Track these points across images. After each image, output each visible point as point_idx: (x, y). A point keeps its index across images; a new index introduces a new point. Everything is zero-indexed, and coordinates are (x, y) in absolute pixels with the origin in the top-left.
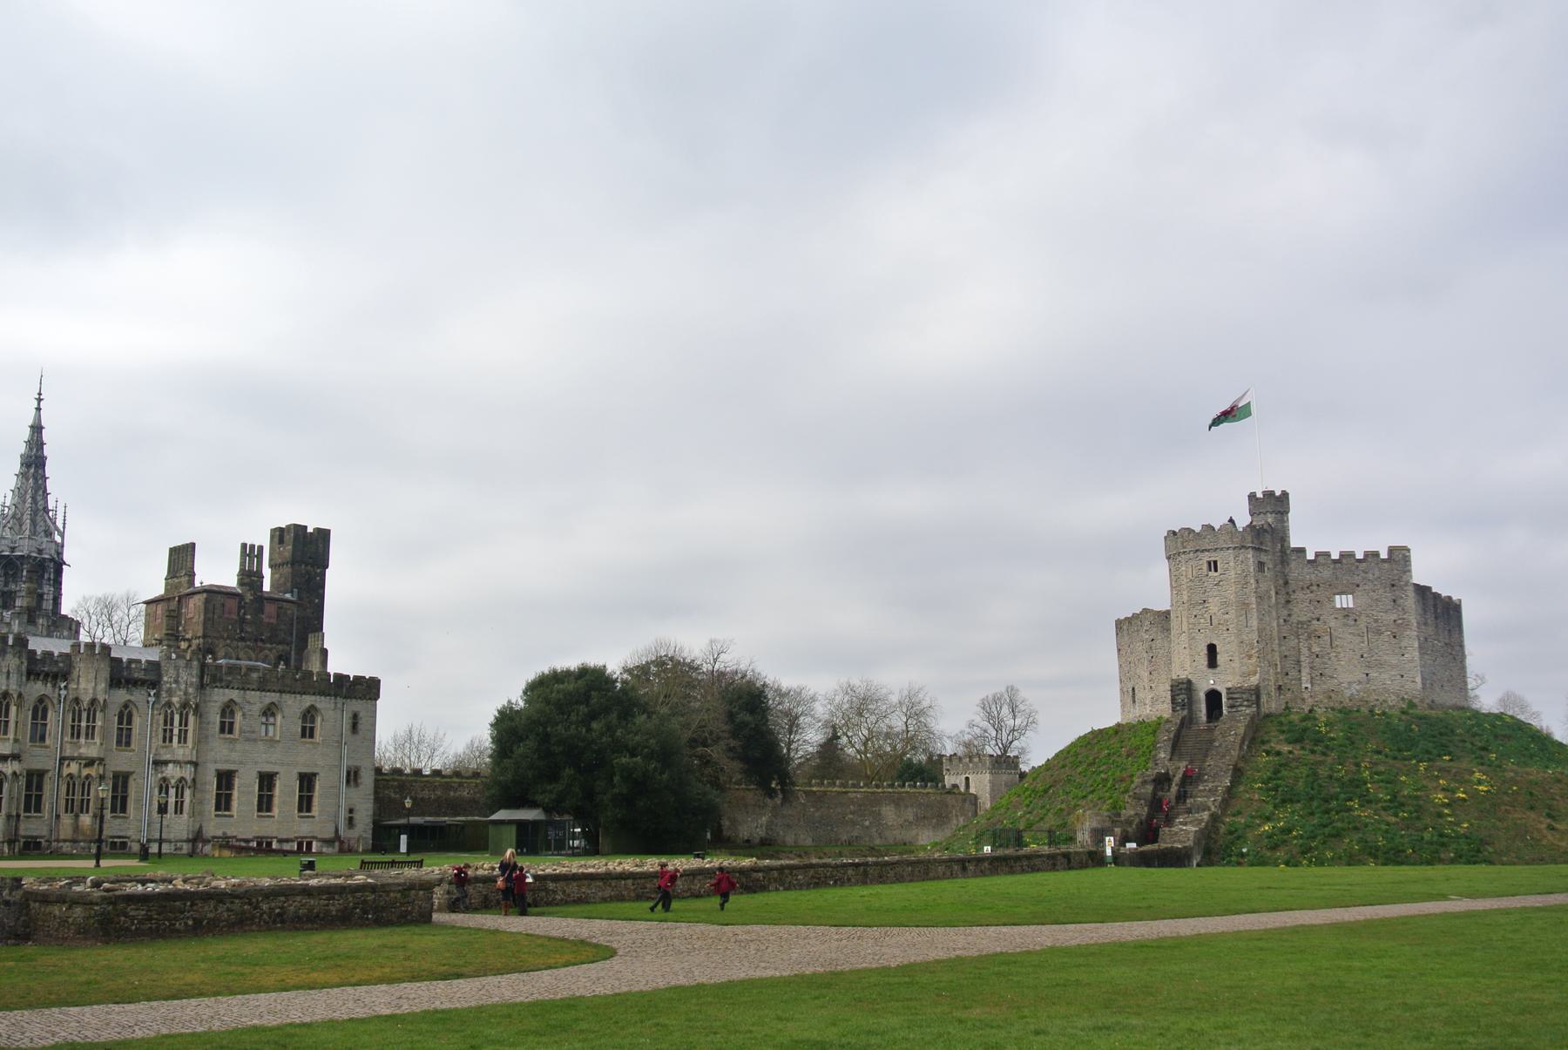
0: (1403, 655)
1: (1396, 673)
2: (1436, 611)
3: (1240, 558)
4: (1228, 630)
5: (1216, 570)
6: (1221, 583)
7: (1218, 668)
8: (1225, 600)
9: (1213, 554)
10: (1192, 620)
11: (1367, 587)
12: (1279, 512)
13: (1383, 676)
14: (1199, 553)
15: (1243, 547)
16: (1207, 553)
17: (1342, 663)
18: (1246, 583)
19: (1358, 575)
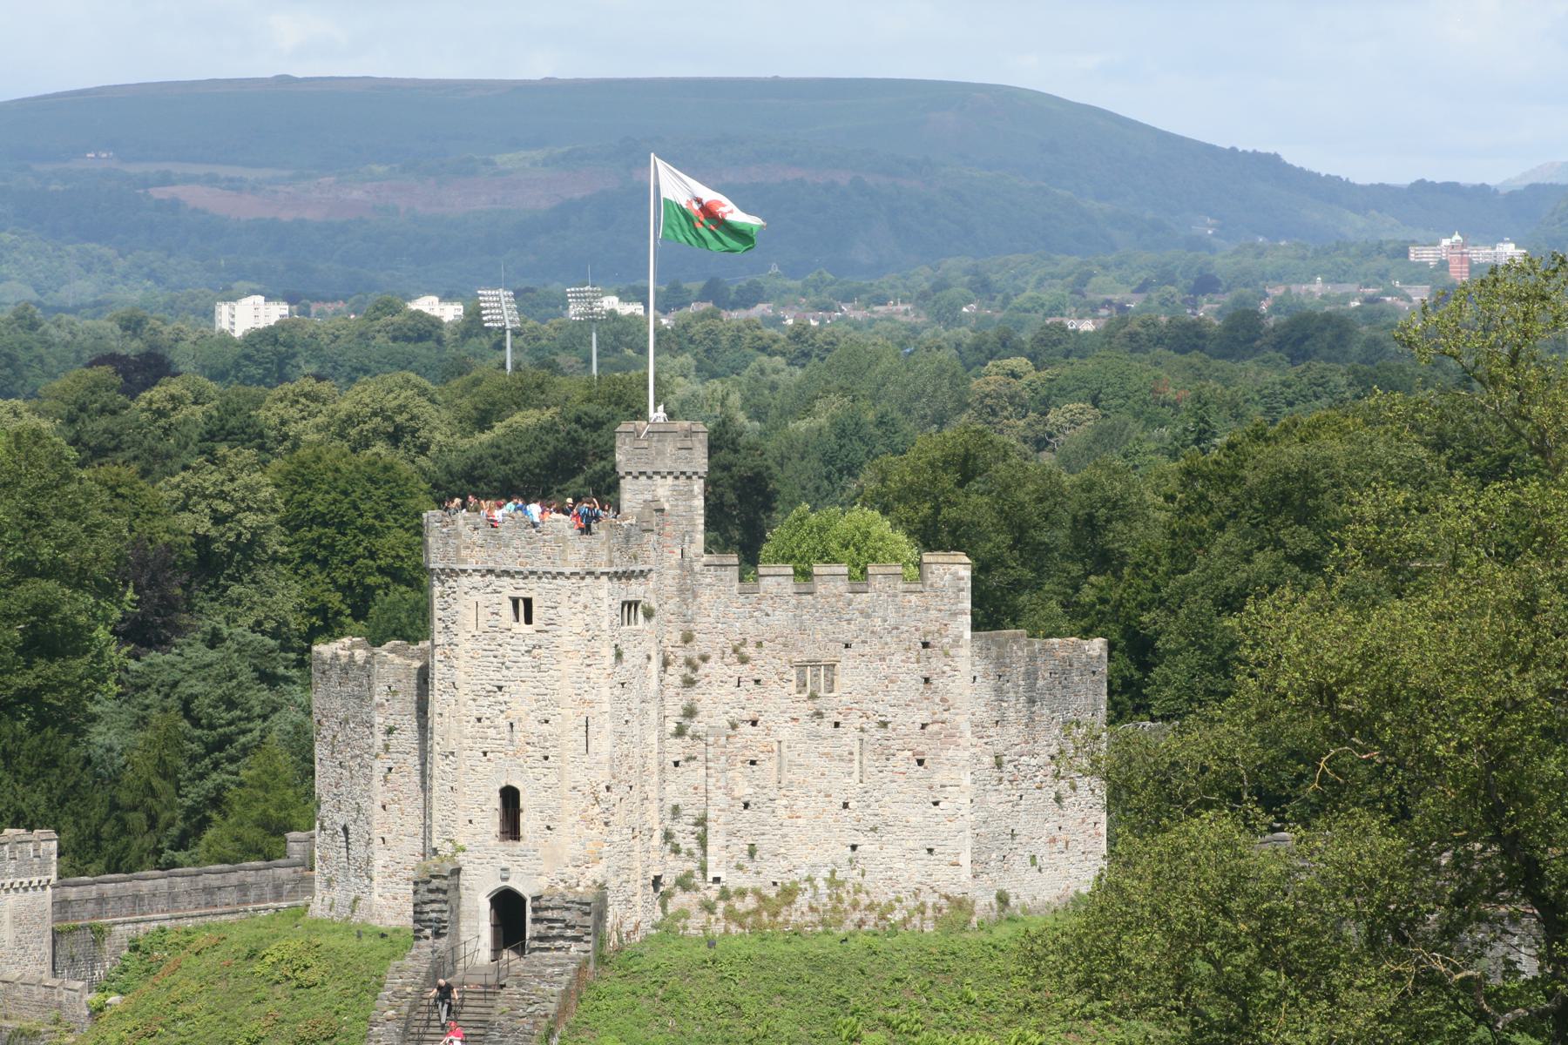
0: (936, 804)
1: (917, 846)
2: (1031, 687)
3: (582, 599)
4: (546, 758)
5: (529, 620)
6: (535, 652)
7: (521, 843)
8: (543, 691)
9: (520, 582)
10: (470, 729)
11: (867, 649)
12: (683, 473)
13: (891, 850)
14: (490, 578)
15: (590, 573)
16: (513, 581)
17: (800, 821)
18: (594, 654)
19: (849, 621)
